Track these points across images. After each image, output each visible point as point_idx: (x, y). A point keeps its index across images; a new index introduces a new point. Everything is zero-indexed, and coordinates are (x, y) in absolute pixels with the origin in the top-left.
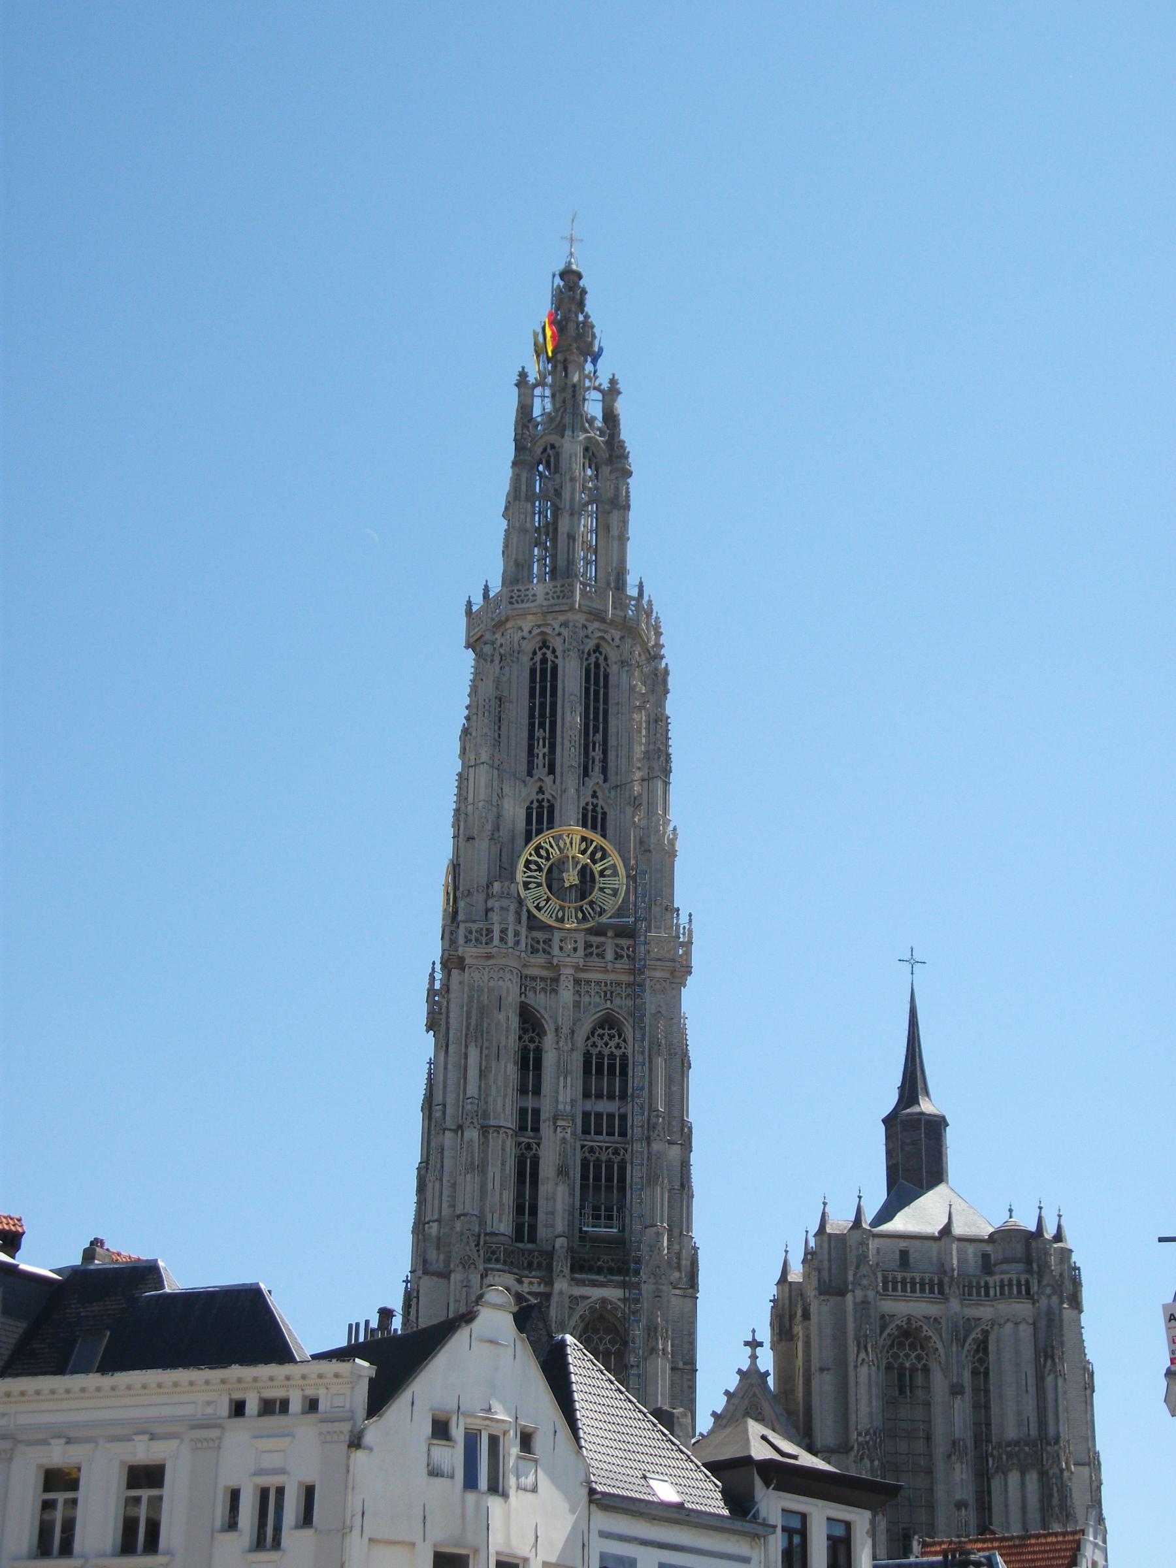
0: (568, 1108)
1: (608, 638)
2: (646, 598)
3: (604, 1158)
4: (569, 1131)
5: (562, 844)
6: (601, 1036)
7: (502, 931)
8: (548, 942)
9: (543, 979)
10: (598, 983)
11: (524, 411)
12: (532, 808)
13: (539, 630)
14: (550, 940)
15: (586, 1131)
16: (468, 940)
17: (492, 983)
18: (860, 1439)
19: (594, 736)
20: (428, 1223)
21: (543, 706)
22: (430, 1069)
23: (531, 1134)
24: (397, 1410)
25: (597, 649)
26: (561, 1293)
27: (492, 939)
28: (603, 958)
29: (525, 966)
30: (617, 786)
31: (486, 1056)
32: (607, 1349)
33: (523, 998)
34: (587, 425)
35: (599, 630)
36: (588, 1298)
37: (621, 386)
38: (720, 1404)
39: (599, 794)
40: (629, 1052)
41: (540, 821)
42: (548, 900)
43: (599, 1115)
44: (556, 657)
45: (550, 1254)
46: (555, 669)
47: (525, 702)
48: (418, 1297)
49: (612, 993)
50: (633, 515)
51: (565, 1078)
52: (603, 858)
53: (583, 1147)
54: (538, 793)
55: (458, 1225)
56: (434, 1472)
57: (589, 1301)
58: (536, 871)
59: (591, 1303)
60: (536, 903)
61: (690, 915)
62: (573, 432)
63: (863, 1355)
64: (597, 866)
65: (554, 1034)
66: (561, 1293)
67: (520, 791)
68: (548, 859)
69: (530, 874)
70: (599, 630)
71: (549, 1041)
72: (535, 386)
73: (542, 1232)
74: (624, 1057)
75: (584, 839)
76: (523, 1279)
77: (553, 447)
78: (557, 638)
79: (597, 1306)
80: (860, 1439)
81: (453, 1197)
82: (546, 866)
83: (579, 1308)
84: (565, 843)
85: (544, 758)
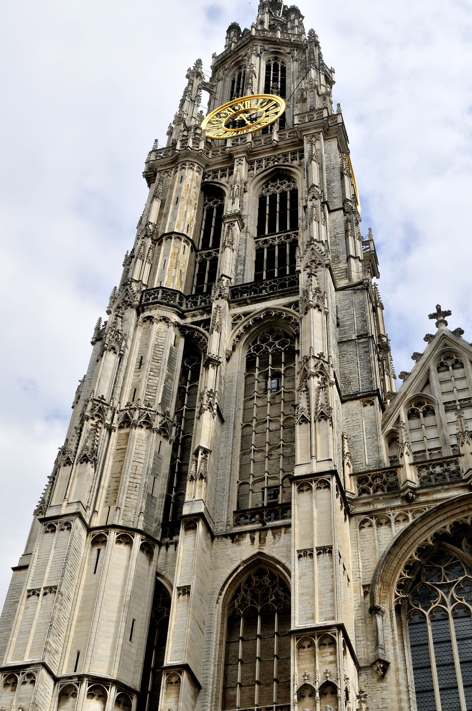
1: (282, 51)
10: (268, 159)
25: (276, 58)
29: (207, 166)
32: (277, 350)
33: (206, 180)
36: (251, 313)
53: (256, 242)
57: (252, 314)
59: (254, 315)
65: (229, 189)
70: (274, 48)
76: (186, 314)
79: (262, 317)
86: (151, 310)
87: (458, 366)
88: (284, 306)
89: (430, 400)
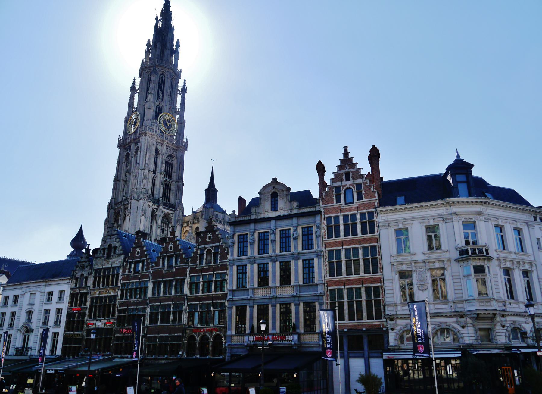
6: (169, 158)
9: (160, 143)
10: (170, 147)
11: (156, 25)
17: (152, 141)
21: (161, 87)
27: (153, 131)
40: (173, 163)
41: (159, 110)
46: (164, 80)
81: (140, 184)
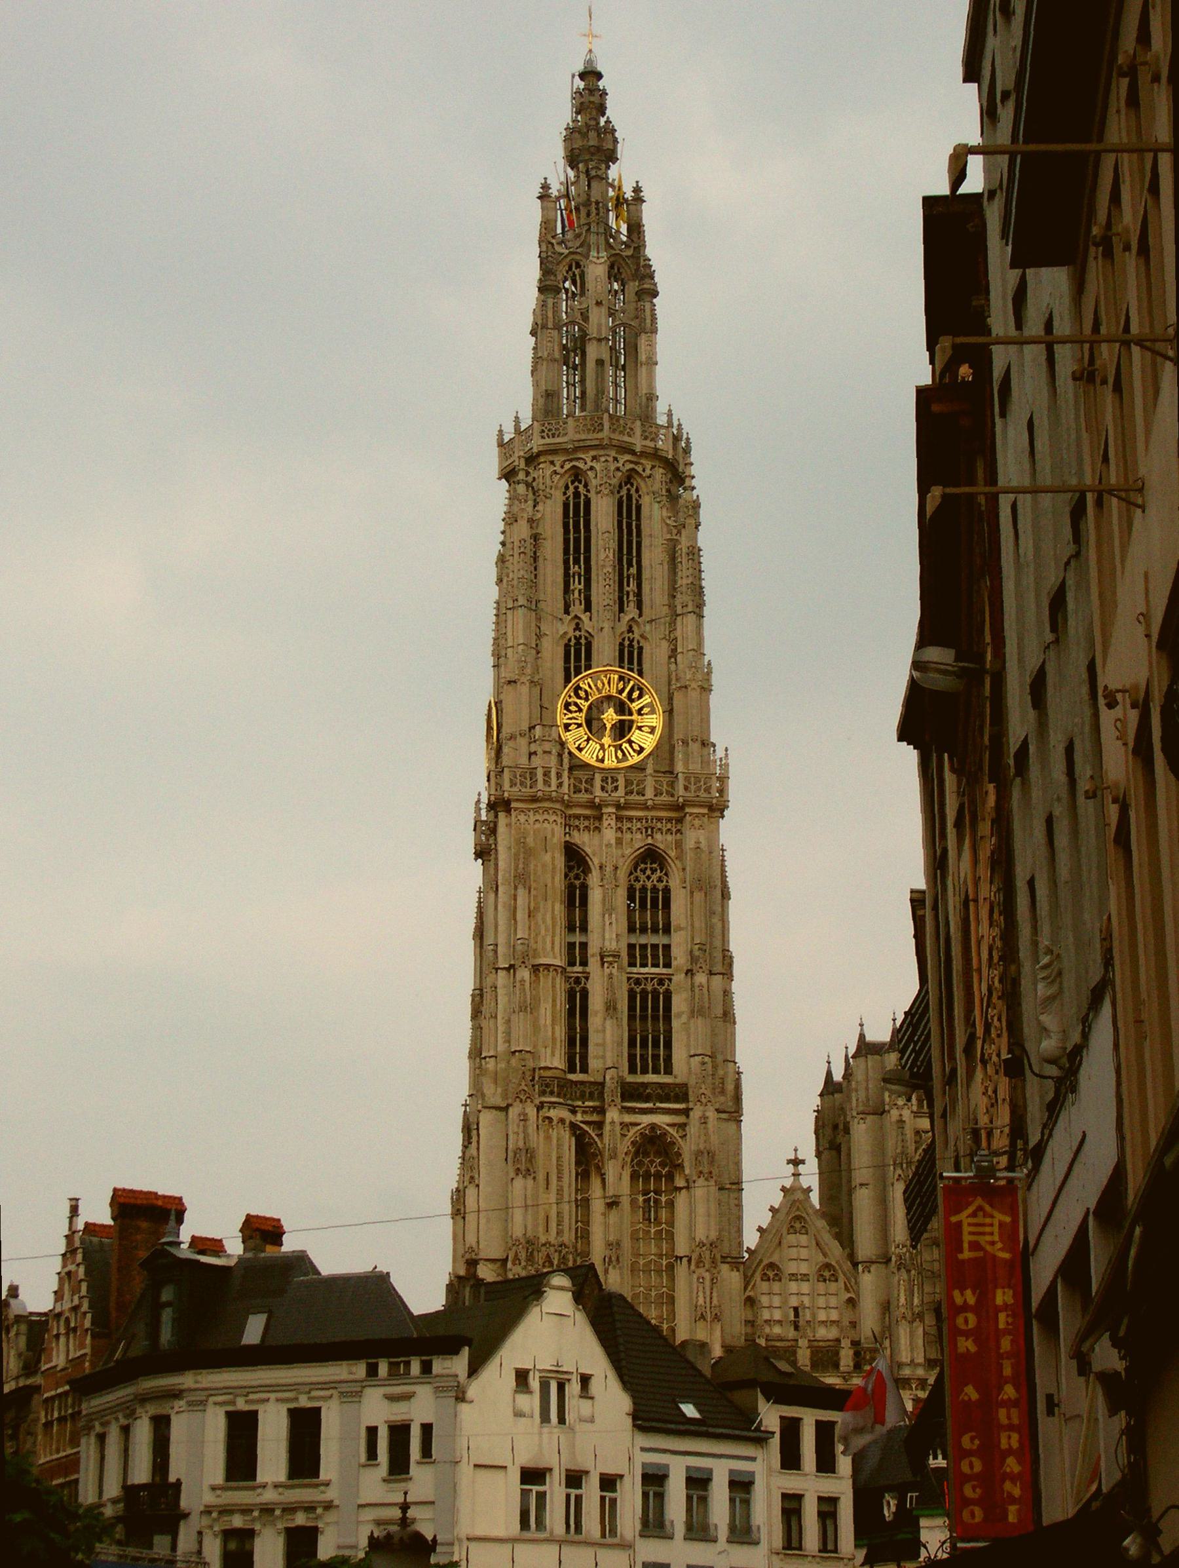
0: (614, 944)
1: (640, 469)
2: (676, 423)
3: (649, 988)
4: (616, 965)
5: (600, 684)
6: (644, 871)
7: (545, 775)
8: (590, 781)
9: (587, 818)
10: (639, 819)
12: (570, 646)
13: (571, 464)
14: (592, 779)
15: (632, 964)
16: (513, 784)
18: (898, 1251)
19: (628, 570)
20: (485, 1058)
21: (577, 540)
22: (480, 898)
23: (580, 969)
24: (490, 1372)
26: (613, 1122)
28: (643, 795)
29: (568, 806)
30: (652, 621)
31: (534, 896)
32: (658, 1171)
33: (568, 838)
34: (611, 240)
35: (631, 462)
36: (639, 1124)
37: (645, 194)
38: (765, 1220)
39: (635, 628)
40: (672, 884)
41: (578, 658)
42: (588, 740)
43: (643, 947)
44: (588, 491)
45: (603, 1084)
47: (560, 539)
48: (478, 1129)
49: (652, 829)
50: (661, 338)
51: (610, 915)
52: (640, 697)
53: (629, 979)
54: (575, 630)
55: (514, 1062)
56: (518, 1414)
57: (639, 1127)
58: (576, 712)
60: (577, 743)
61: (726, 750)
62: (598, 253)
63: (899, 1171)
64: (634, 704)
66: (613, 1122)
67: (557, 630)
68: (587, 699)
69: (570, 716)
71: (594, 879)
72: (558, 198)
73: (594, 1063)
74: (667, 890)
75: (621, 678)
77: (578, 266)
78: (589, 473)
80: (898, 1251)
82: (585, 705)
83: (630, 1134)
84: (603, 684)
85: (580, 595)
86: (549, 1108)
87: (803, 1231)
88: (668, 1125)
89: (779, 1269)
